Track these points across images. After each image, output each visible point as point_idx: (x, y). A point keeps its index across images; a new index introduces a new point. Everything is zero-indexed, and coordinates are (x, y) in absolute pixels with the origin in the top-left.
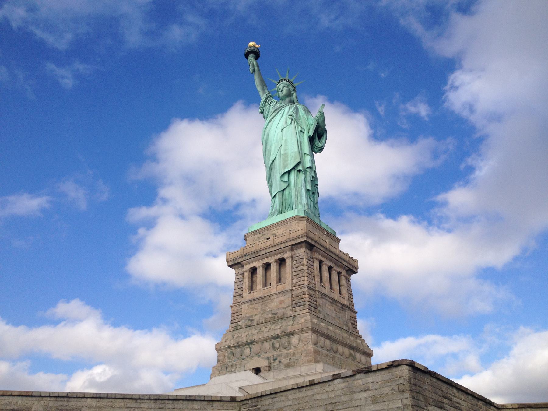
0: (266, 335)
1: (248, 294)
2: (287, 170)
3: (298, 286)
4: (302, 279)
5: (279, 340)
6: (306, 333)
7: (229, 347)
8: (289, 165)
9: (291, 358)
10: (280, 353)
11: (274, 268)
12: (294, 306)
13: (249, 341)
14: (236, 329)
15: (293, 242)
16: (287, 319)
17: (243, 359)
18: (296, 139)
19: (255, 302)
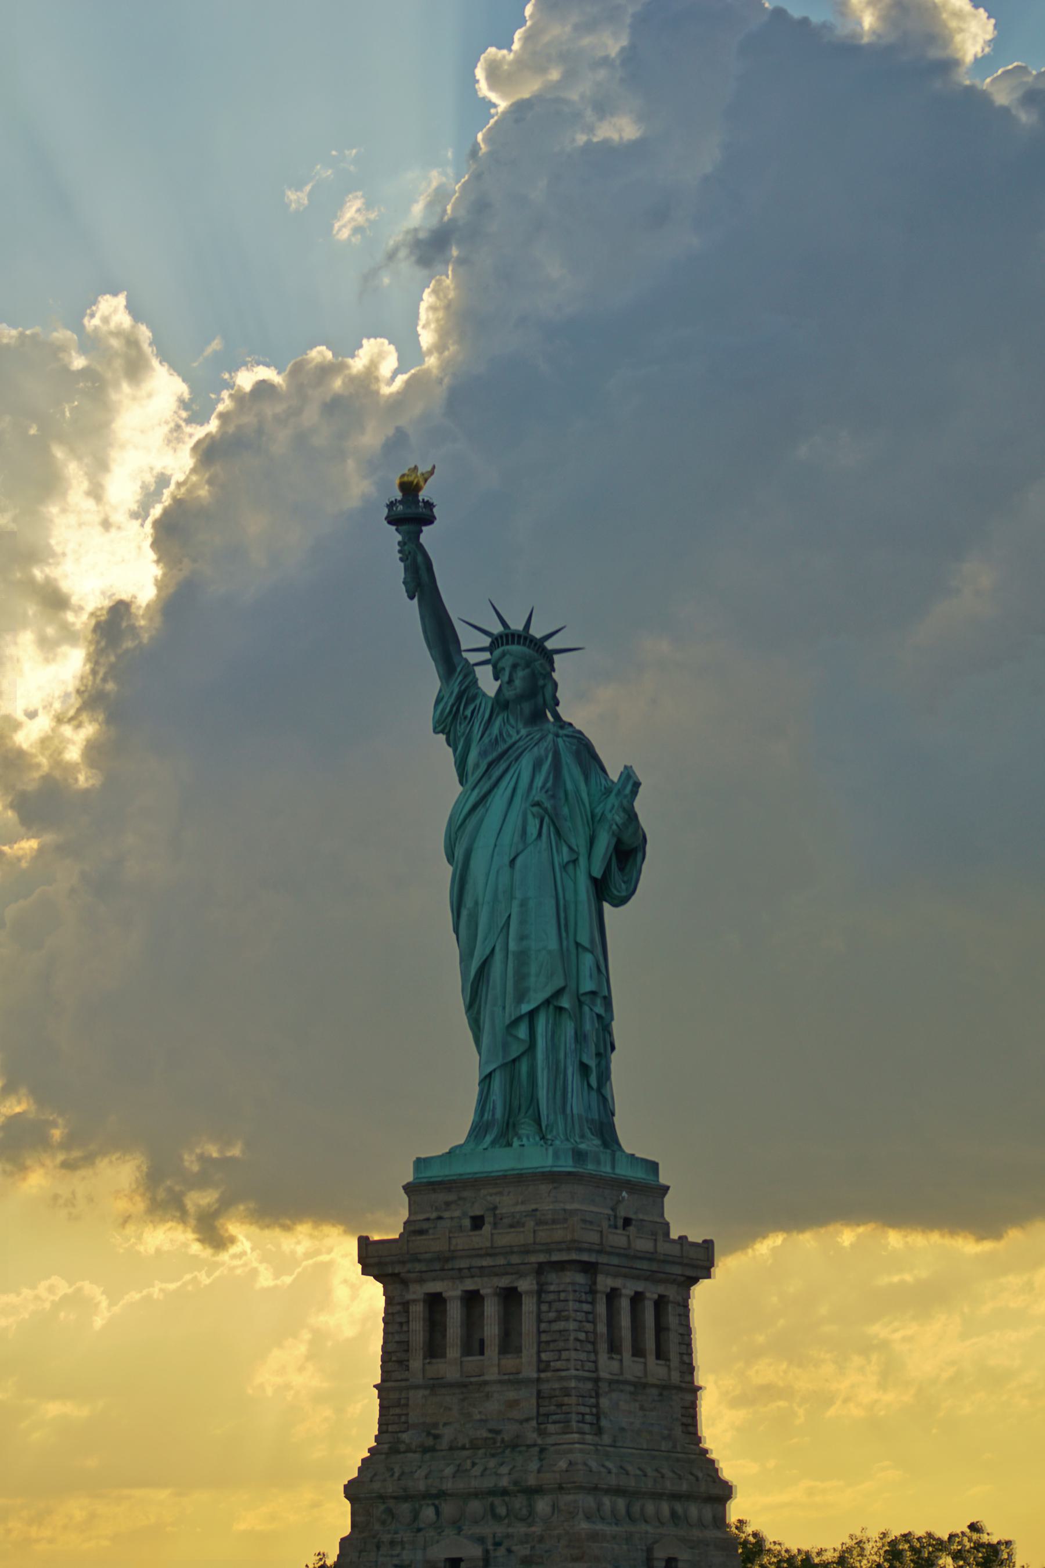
0: (475, 1484)
1: (424, 1364)
2: (525, 1008)
3: (554, 1371)
4: (565, 1355)
5: (507, 1498)
6: (570, 1494)
7: (382, 1498)
10: (510, 1530)
11: (491, 1309)
12: (541, 1419)
13: (434, 1491)
14: (394, 1451)
15: (542, 1258)
17: (419, 1530)
18: (553, 902)
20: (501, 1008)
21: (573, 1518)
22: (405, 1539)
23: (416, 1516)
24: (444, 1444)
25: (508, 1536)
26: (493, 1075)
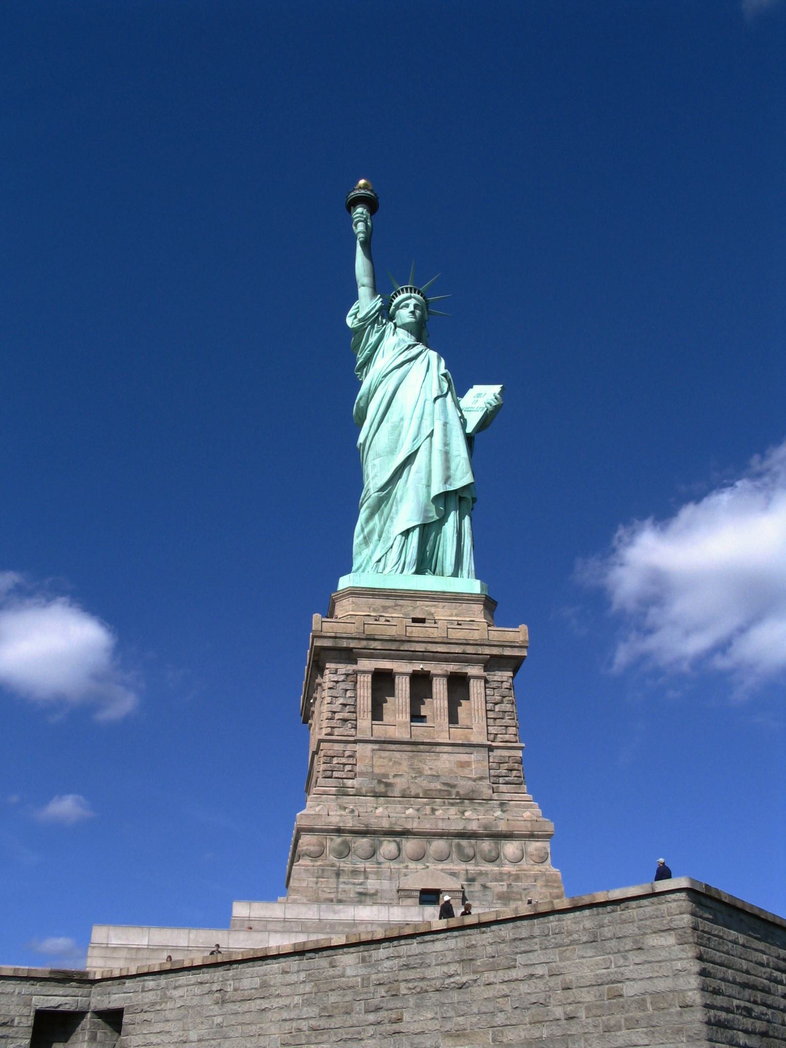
0: (442, 826)
3: (501, 742)
4: (512, 730)
5: (473, 841)
7: (339, 831)
8: (451, 479)
9: (510, 884)
11: (440, 687)
12: (492, 779)
13: (398, 829)
15: (495, 651)
16: (487, 803)
19: (393, 747)
20: (424, 486)
21: (542, 863)
22: (367, 869)
23: (374, 853)
24: (397, 792)
25: (481, 873)
26: (412, 529)
